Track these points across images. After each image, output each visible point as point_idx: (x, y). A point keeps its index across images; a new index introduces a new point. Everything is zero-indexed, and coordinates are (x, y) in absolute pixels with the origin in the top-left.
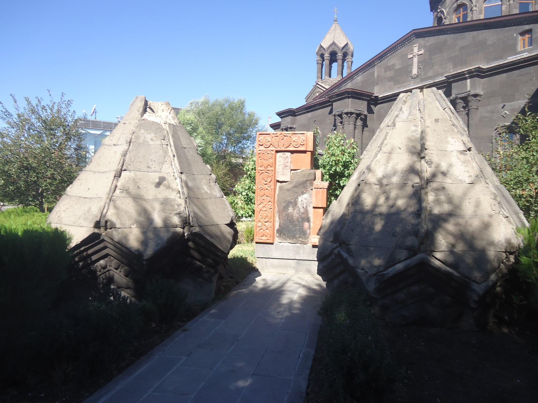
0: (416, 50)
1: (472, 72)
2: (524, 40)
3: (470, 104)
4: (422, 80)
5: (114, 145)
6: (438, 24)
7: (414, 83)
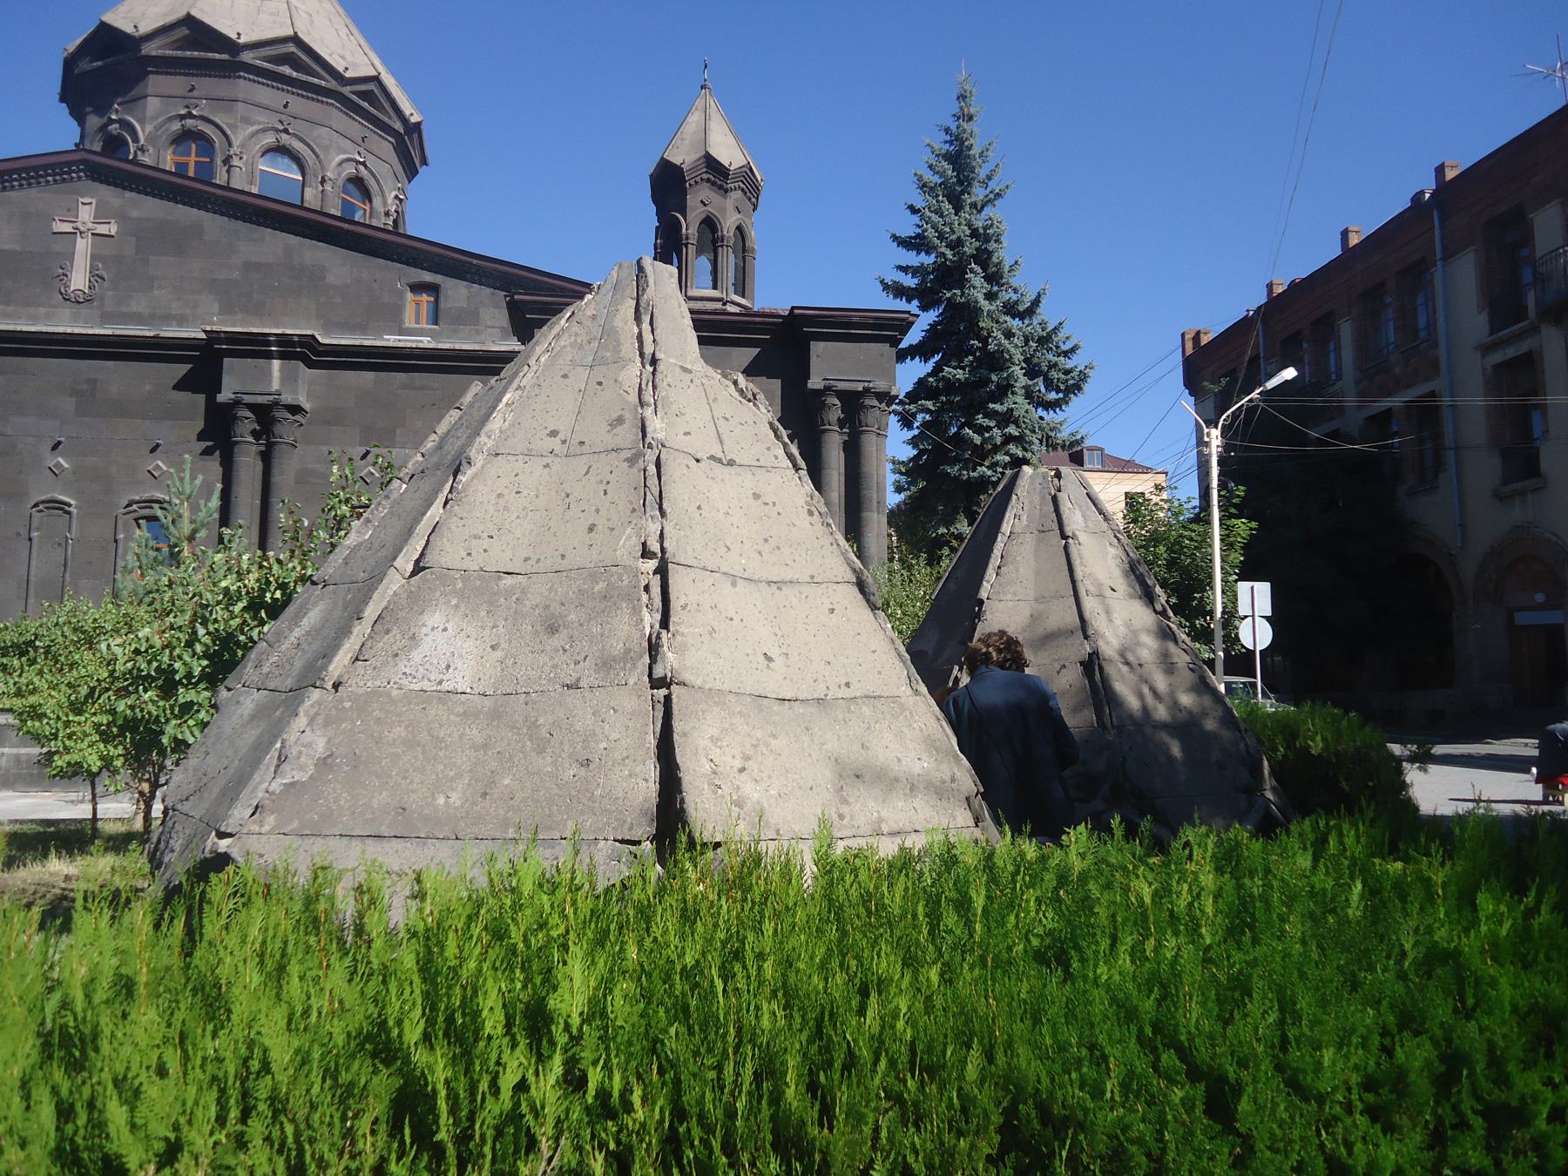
0: (86, 214)
1: (293, 344)
2: (417, 304)
3: (278, 429)
4: (106, 318)
5: (712, 458)
6: (103, 148)
7: (75, 319)
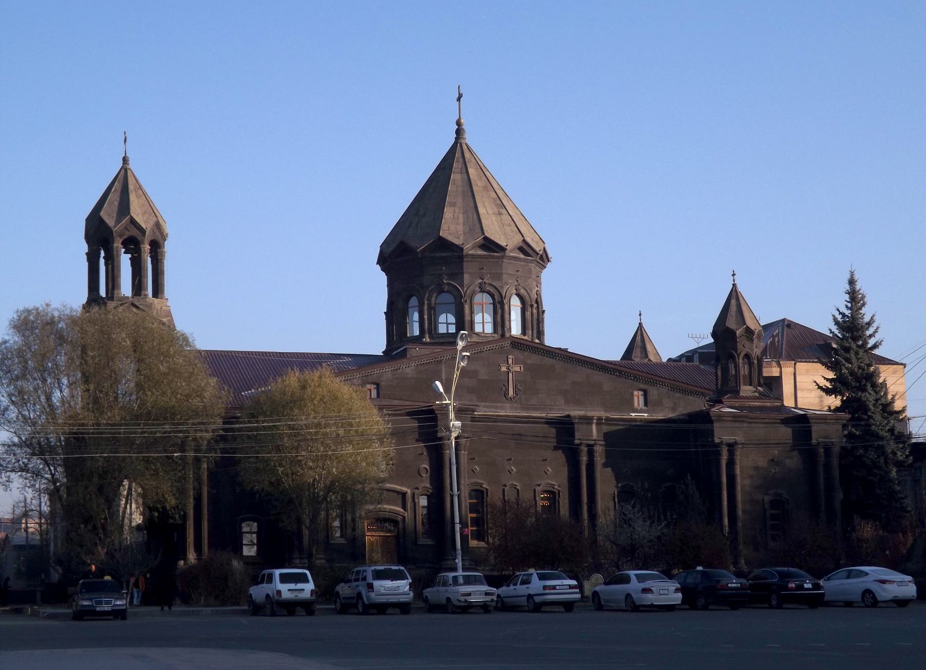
0: (510, 361)
4: (524, 408)
